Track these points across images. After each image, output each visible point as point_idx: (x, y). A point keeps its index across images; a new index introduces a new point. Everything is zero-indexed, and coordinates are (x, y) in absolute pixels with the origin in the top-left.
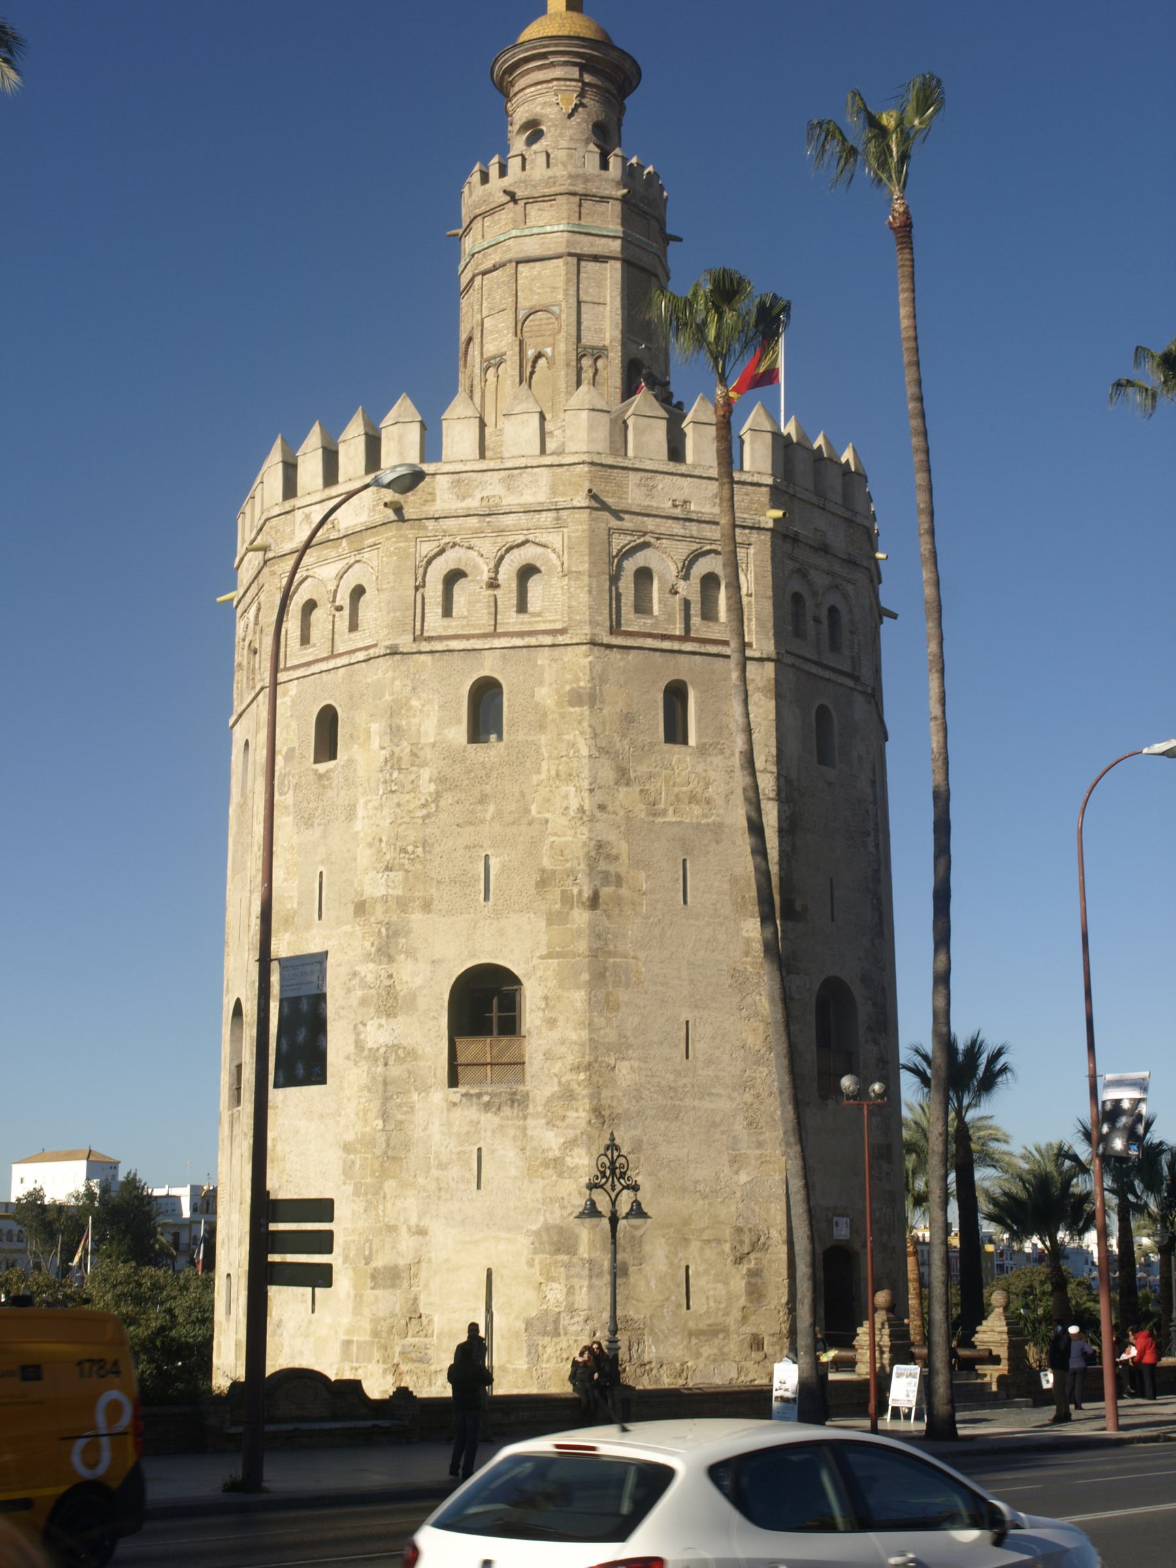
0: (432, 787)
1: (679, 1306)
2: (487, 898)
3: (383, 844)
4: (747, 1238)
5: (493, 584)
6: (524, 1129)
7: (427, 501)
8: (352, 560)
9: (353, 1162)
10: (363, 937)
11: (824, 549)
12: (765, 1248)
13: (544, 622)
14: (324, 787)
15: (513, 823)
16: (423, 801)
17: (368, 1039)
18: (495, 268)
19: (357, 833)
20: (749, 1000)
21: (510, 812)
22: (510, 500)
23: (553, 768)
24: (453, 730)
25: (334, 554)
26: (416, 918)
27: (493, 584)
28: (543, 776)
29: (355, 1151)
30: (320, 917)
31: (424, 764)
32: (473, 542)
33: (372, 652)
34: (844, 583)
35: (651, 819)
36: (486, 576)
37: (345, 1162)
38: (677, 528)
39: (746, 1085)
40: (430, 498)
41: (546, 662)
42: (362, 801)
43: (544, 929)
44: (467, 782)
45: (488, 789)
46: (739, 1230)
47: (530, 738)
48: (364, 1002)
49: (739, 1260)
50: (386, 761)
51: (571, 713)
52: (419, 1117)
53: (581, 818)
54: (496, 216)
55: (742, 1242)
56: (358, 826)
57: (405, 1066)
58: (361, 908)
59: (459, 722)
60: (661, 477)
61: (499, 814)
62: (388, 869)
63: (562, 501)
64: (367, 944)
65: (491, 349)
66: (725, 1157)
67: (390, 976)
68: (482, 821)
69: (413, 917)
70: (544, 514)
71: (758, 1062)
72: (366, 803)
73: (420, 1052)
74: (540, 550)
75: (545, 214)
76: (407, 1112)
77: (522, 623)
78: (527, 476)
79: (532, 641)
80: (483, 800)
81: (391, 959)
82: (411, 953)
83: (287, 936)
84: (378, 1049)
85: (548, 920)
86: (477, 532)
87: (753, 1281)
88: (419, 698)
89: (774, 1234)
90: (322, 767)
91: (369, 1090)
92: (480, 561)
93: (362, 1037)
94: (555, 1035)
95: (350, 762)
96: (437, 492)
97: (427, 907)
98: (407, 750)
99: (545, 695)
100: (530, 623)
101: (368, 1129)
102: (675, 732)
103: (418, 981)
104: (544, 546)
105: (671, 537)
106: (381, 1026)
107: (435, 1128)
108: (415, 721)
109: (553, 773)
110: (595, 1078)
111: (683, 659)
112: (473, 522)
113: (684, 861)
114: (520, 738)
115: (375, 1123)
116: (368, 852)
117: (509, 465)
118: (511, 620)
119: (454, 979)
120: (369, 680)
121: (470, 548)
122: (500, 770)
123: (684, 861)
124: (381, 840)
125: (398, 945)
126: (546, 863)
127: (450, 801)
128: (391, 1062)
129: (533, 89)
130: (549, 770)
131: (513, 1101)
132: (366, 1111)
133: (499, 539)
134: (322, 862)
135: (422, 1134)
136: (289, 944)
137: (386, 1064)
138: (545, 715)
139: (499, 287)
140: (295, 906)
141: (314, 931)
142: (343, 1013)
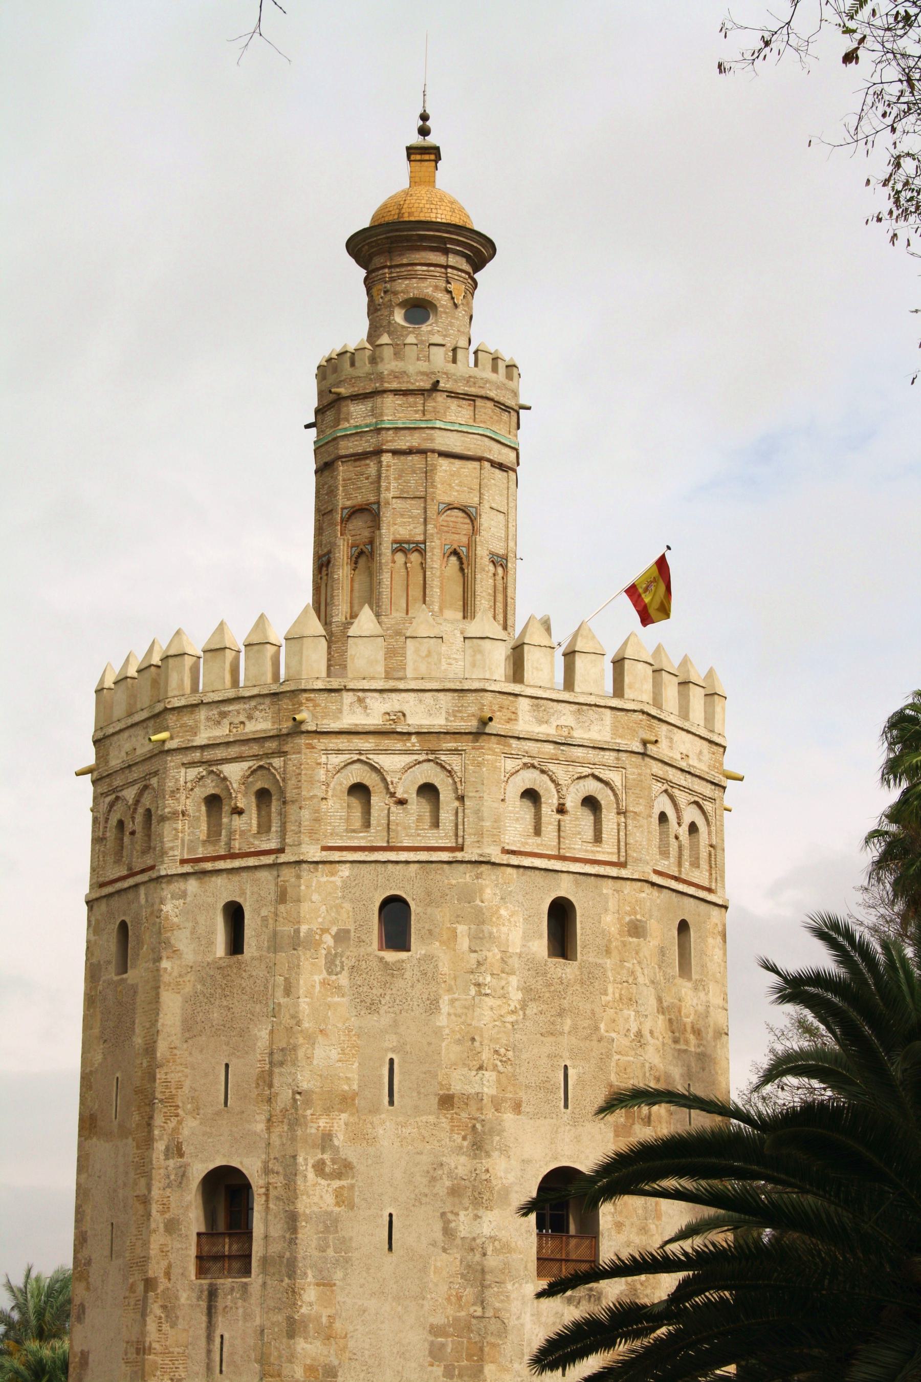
0: (520, 995)
2: (566, 1106)
3: (477, 1044)
5: (561, 810)
7: (510, 719)
8: (421, 758)
9: (443, 1346)
10: (452, 1130)
13: (603, 853)
14: (393, 975)
15: (586, 1038)
16: (512, 1008)
17: (461, 1228)
18: (410, 452)
19: (443, 1027)
21: (584, 1028)
22: (579, 735)
23: (617, 991)
24: (536, 943)
25: (399, 746)
26: (508, 1117)
27: (561, 810)
28: (609, 998)
29: (446, 1335)
30: (391, 1103)
31: (513, 973)
32: (552, 767)
33: (459, 856)
36: (555, 802)
37: (432, 1344)
40: (513, 717)
41: (610, 892)
42: (445, 999)
43: (612, 1140)
44: (547, 995)
45: (565, 1003)
47: (599, 961)
48: (454, 1192)
50: (479, 964)
51: (630, 943)
52: (515, 1306)
53: (640, 1042)
54: (411, 399)
56: (442, 1020)
57: (501, 1257)
58: (447, 1101)
59: (541, 936)
61: (575, 1028)
62: (481, 1068)
63: (623, 743)
64: (458, 1138)
65: (403, 532)
67: (487, 1171)
68: (562, 1033)
69: (505, 1116)
70: (607, 753)
72: (452, 1001)
73: (513, 1245)
74: (600, 785)
75: (464, 412)
76: (502, 1301)
77: (586, 851)
78: (592, 713)
79: (602, 870)
80: (561, 1013)
81: (488, 1155)
82: (504, 1150)
83: (344, 1116)
84: (474, 1239)
85: (615, 1131)
86: (555, 759)
88: (507, 908)
90: (391, 956)
91: (463, 1276)
92: (552, 786)
93: (453, 1225)
94: (622, 1238)
95: (429, 958)
96: (520, 713)
97: (517, 1107)
98: (498, 957)
99: (610, 922)
100: (592, 852)
101: (463, 1314)
103: (511, 1178)
104: (606, 783)
105: (681, 788)
106: (477, 1217)
107: (527, 1319)
108: (504, 929)
109: (617, 995)
112: (550, 748)
114: (591, 959)
115: (472, 1309)
116: (457, 1048)
117: (581, 700)
118: (577, 847)
119: (540, 1179)
120: (454, 882)
121: (543, 772)
122: (574, 988)
124: (473, 1039)
125: (492, 1142)
126: (613, 1078)
127: (535, 1011)
128: (489, 1253)
129: (425, 268)
130: (614, 994)
131: (590, 1297)
132: (459, 1298)
133: (570, 769)
134: (393, 1050)
135: (516, 1322)
136: (346, 1124)
137: (484, 1255)
138: (610, 941)
139: (414, 472)
140: (355, 1087)
141: (383, 1116)
142: (424, 1200)
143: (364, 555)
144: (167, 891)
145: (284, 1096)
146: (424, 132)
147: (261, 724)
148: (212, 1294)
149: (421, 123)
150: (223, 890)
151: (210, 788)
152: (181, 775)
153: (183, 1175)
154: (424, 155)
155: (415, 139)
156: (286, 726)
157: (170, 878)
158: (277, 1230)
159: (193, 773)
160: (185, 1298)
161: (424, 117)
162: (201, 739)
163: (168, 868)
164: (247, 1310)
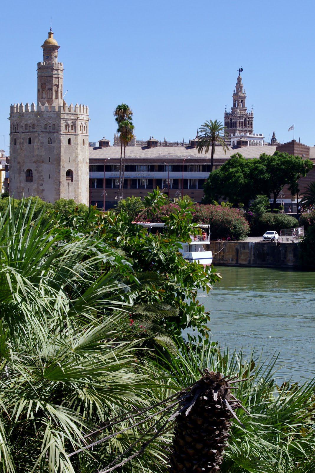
143: (57, 91)
144: (61, 136)
145: (77, 162)
147: (73, 117)
148: (69, 184)
150: (69, 137)
151: (66, 124)
152: (62, 121)
153: (64, 170)
155: (50, 31)
156: (76, 118)
157: (62, 134)
158: (76, 177)
159: (64, 122)
160: (65, 184)
162: (66, 117)
163: (62, 133)
164: (73, 185)
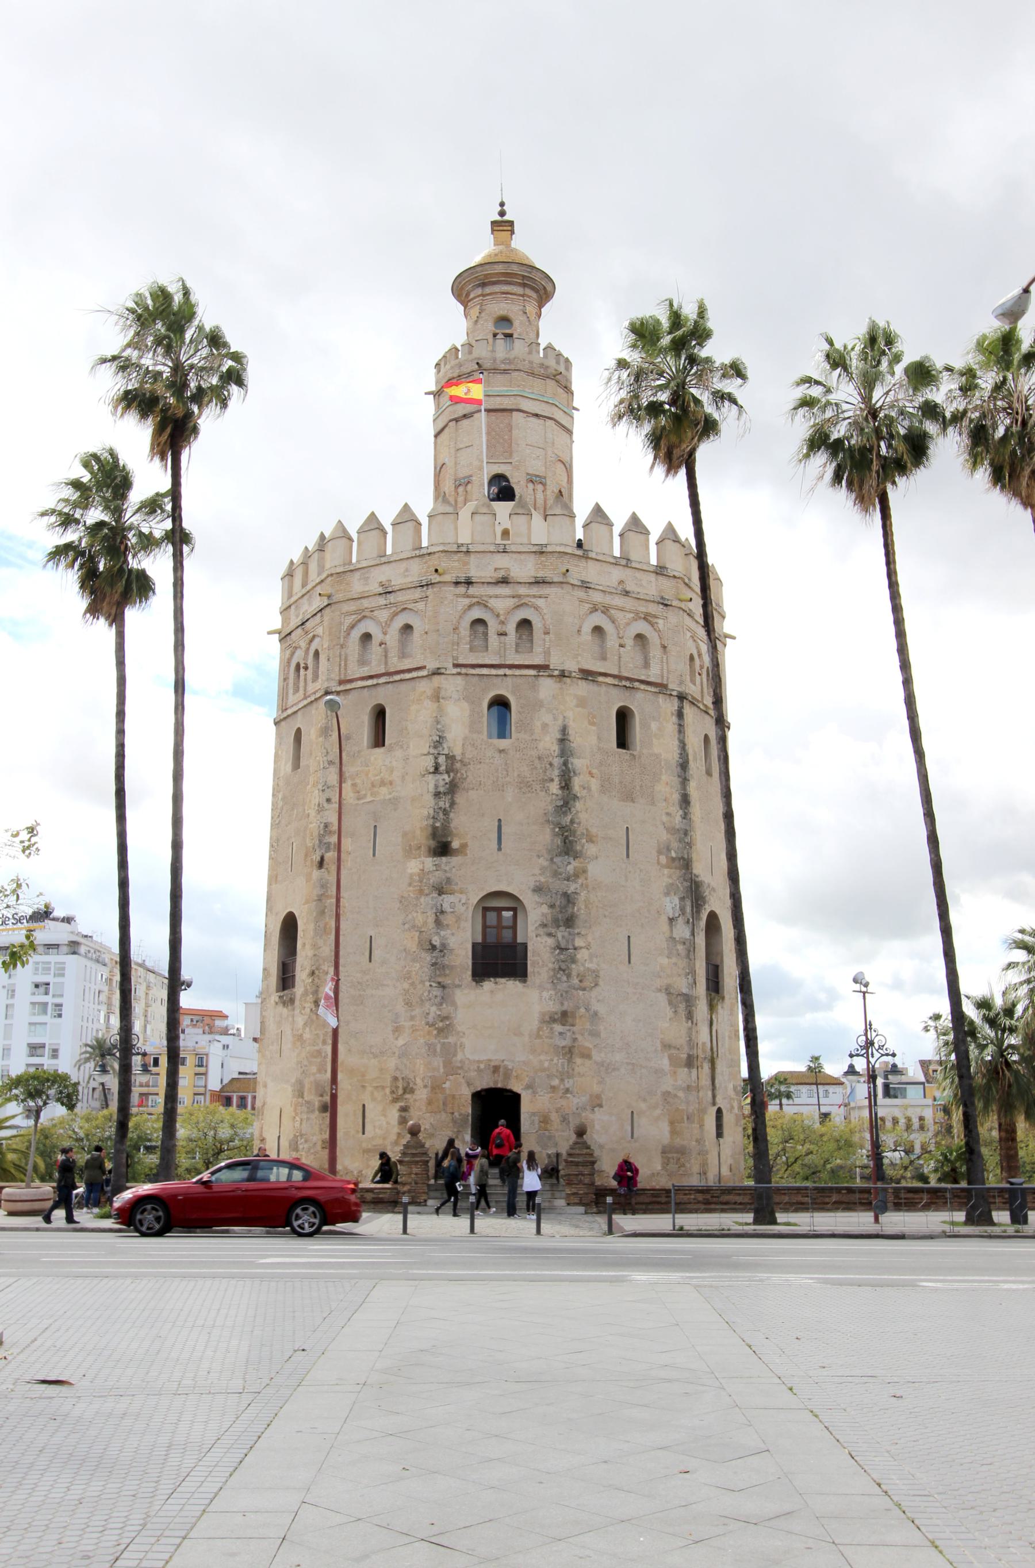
1: (358, 1132)
4: (400, 1084)
6: (293, 1016)
11: (504, 581)
12: (412, 1091)
20: (410, 917)
34: (533, 600)
35: (357, 802)
38: (382, 601)
39: (407, 977)
46: (396, 1079)
49: (395, 1100)
55: (397, 1087)
60: (372, 569)
66: (390, 1028)
71: (414, 960)
87: (403, 1114)
89: (418, 1081)
102: (379, 739)
105: (380, 608)
110: (316, 980)
111: (381, 690)
113: (375, 826)
123: (375, 826)
146: (502, 214)
149: (499, 208)
154: (503, 226)
161: (502, 204)
